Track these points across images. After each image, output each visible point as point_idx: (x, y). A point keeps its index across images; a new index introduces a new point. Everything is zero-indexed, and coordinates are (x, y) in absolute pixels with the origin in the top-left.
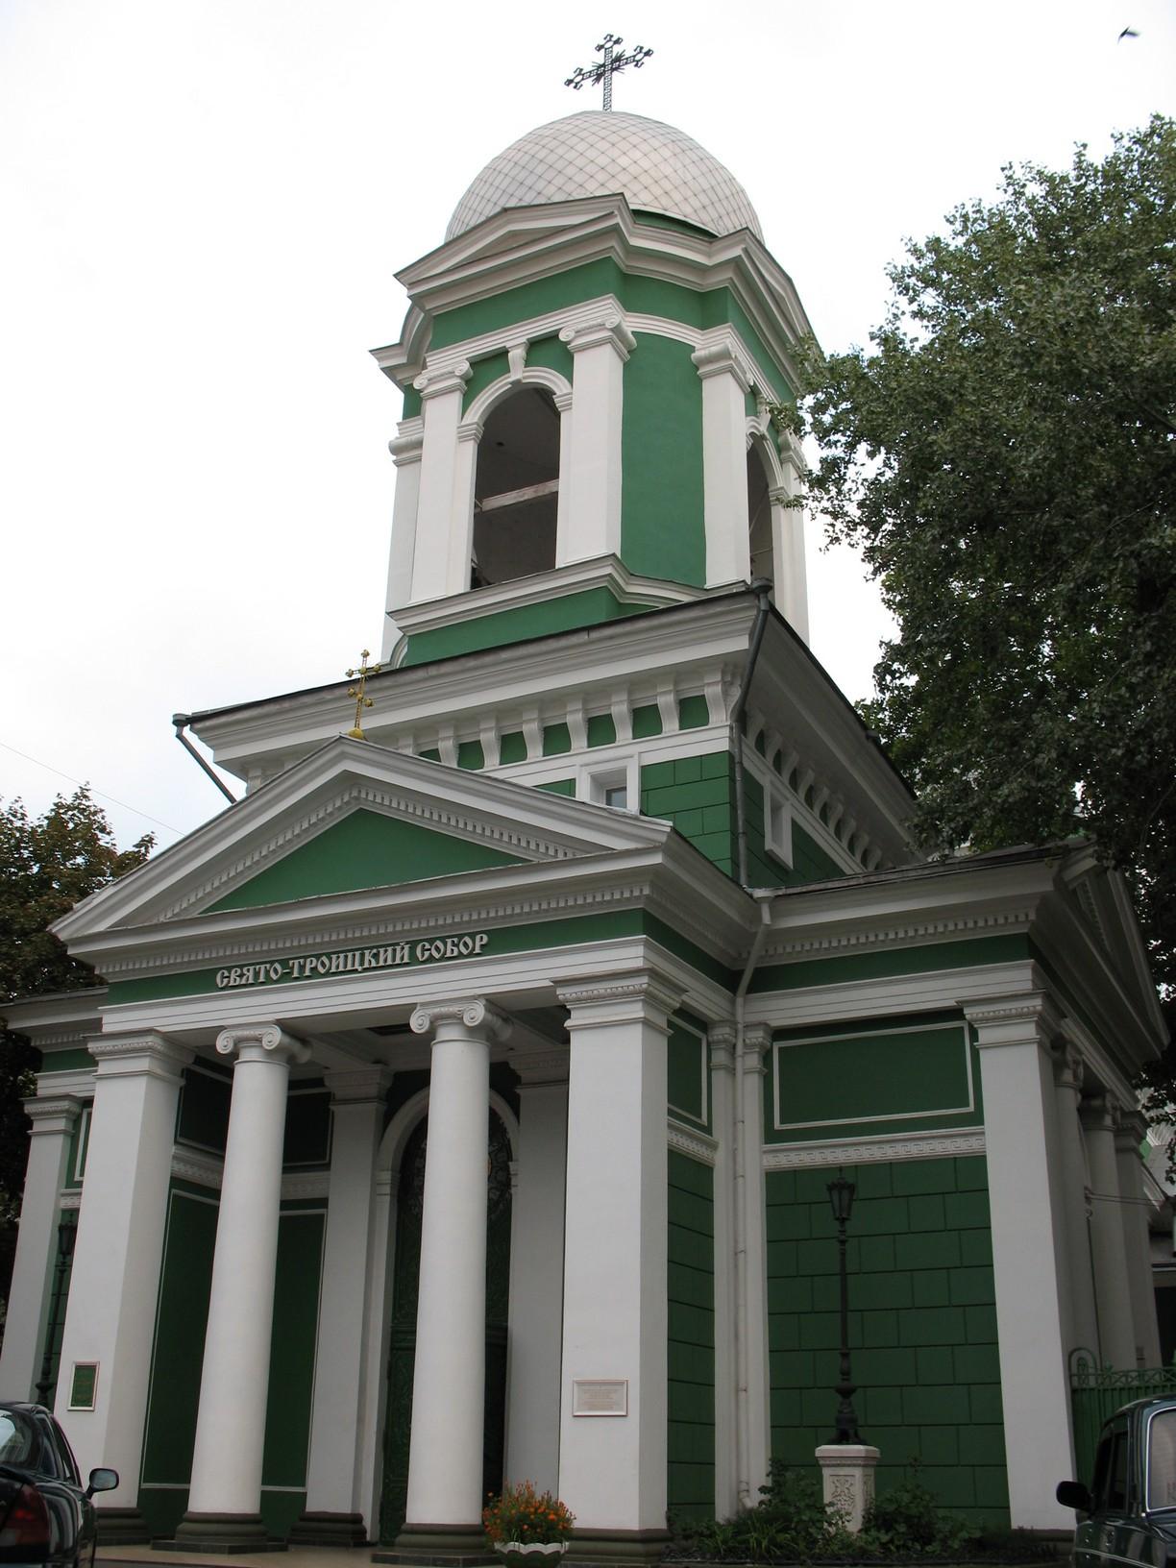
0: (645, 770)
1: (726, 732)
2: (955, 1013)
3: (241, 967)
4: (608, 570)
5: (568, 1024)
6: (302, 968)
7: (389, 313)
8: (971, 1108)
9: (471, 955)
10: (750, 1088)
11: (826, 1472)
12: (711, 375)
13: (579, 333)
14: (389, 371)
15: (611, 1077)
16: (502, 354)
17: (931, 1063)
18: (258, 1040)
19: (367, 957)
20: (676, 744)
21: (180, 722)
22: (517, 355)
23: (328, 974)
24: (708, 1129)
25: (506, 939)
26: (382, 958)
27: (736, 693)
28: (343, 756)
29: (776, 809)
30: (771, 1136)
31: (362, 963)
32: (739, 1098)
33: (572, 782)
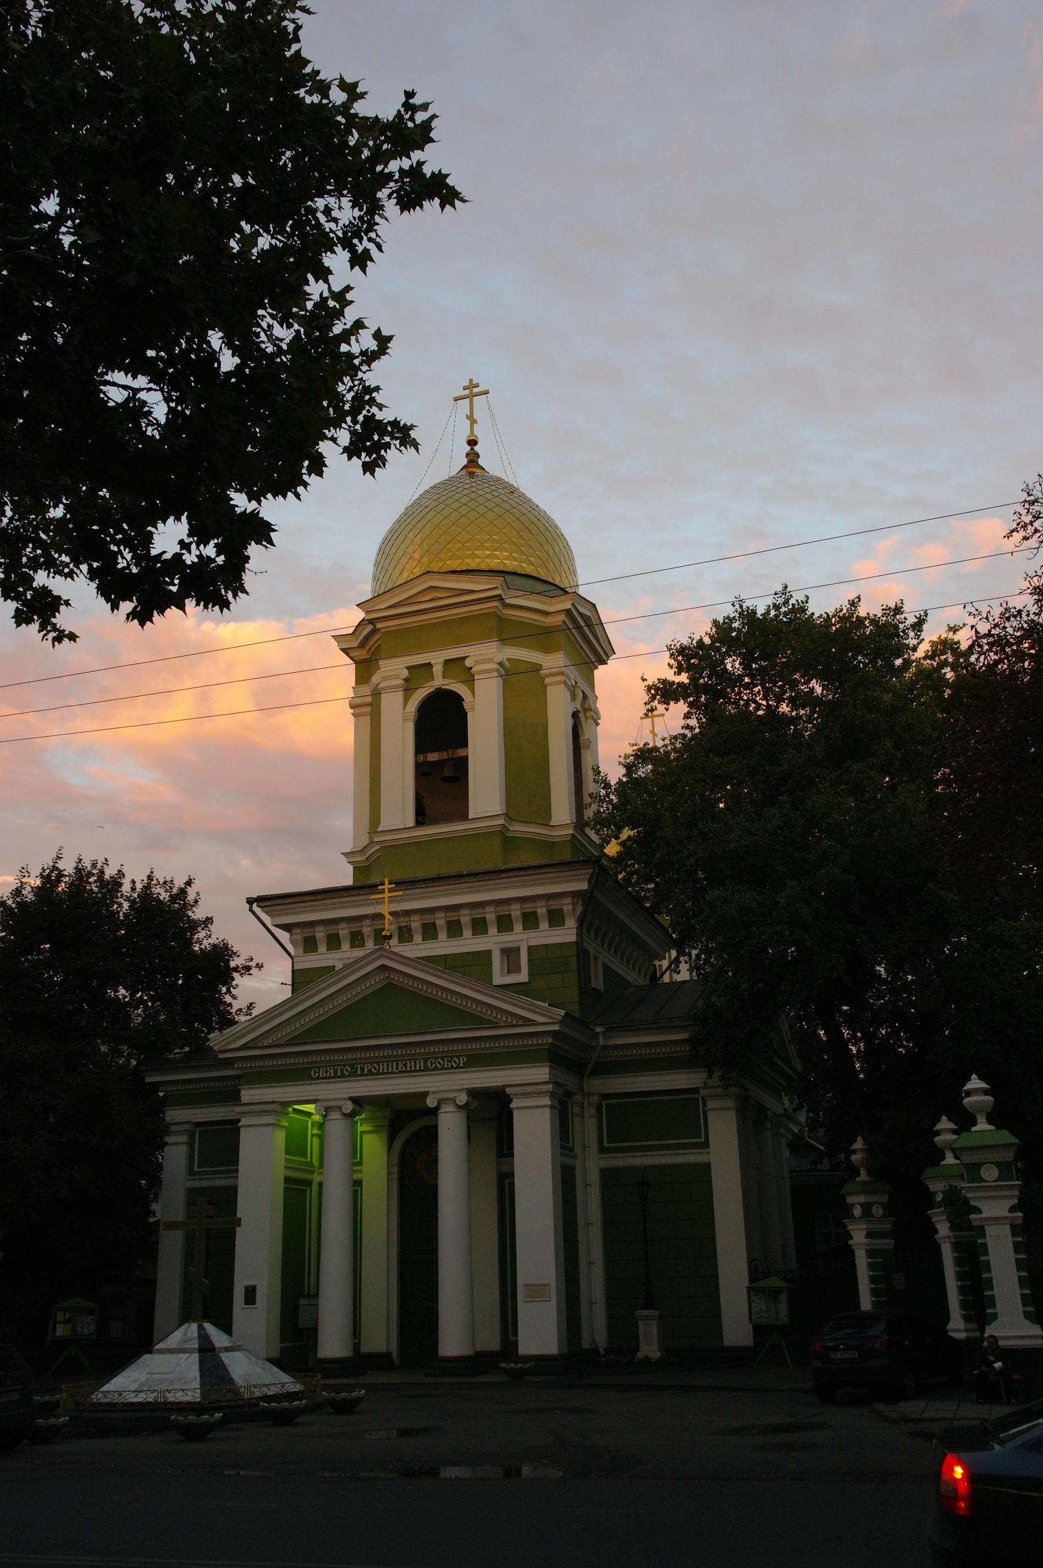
0: (530, 948)
1: (575, 931)
2: (696, 1090)
4: (502, 822)
5: (512, 1105)
6: (362, 1069)
7: (351, 618)
8: (703, 1139)
9: (458, 1067)
10: (592, 1125)
11: (640, 1323)
12: (552, 684)
13: (477, 662)
14: (345, 651)
15: (533, 1129)
16: (429, 666)
17: (682, 1117)
18: (340, 1108)
20: (546, 935)
21: (250, 901)
22: (438, 669)
23: (378, 1073)
24: (572, 1149)
25: (477, 1061)
27: (579, 908)
28: (382, 956)
29: (596, 958)
30: (602, 1150)
31: (397, 1068)
32: (587, 1131)
33: (488, 953)
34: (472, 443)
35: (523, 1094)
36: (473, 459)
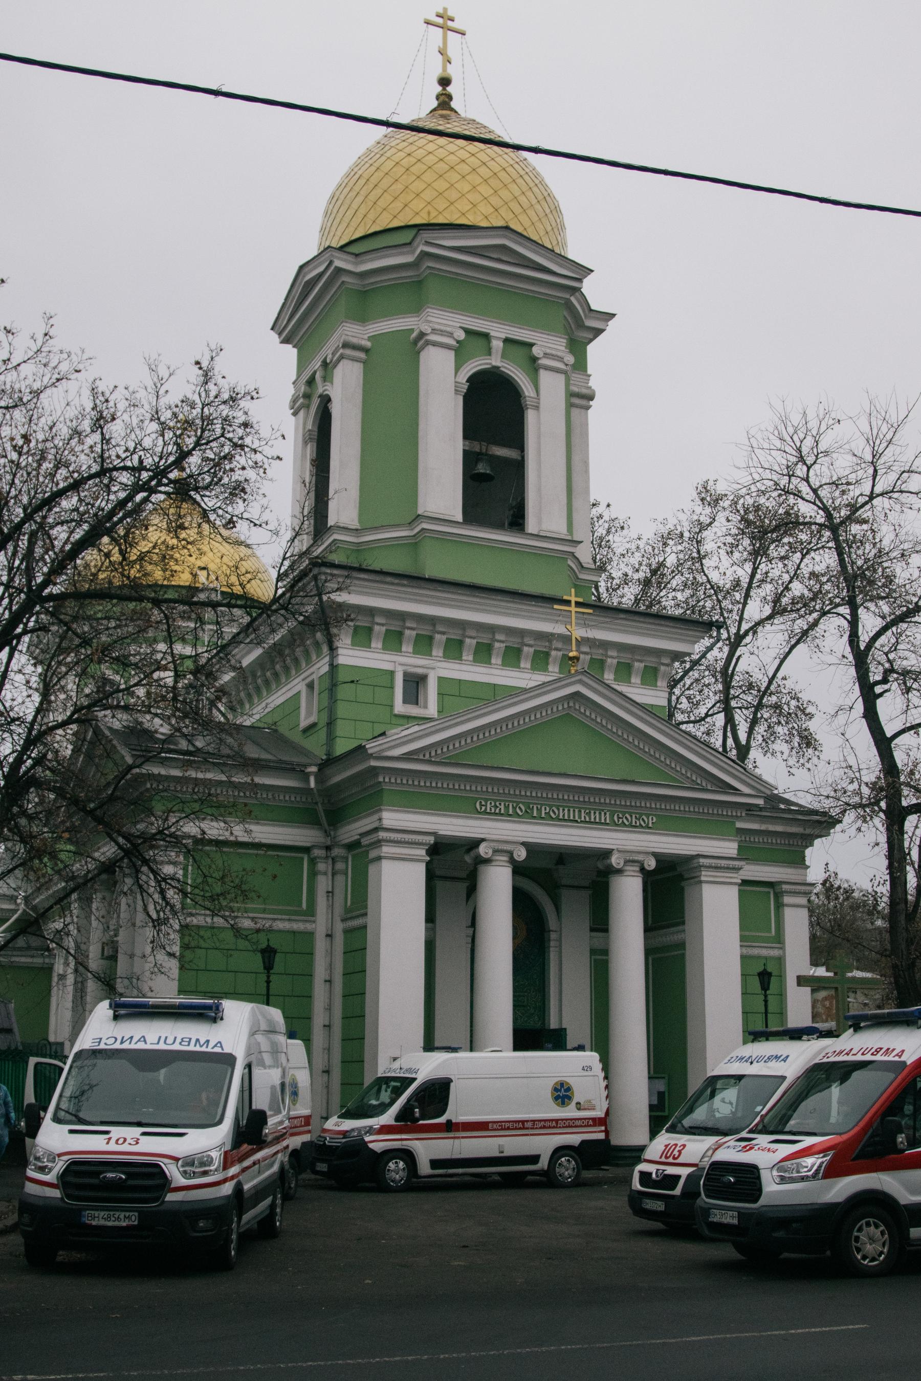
3: (495, 801)
6: (539, 810)
13: (546, 355)
16: (486, 336)
19: (583, 815)
22: (497, 345)
26: (593, 817)
28: (580, 682)
31: (580, 817)
34: (445, 82)
36: (444, 102)
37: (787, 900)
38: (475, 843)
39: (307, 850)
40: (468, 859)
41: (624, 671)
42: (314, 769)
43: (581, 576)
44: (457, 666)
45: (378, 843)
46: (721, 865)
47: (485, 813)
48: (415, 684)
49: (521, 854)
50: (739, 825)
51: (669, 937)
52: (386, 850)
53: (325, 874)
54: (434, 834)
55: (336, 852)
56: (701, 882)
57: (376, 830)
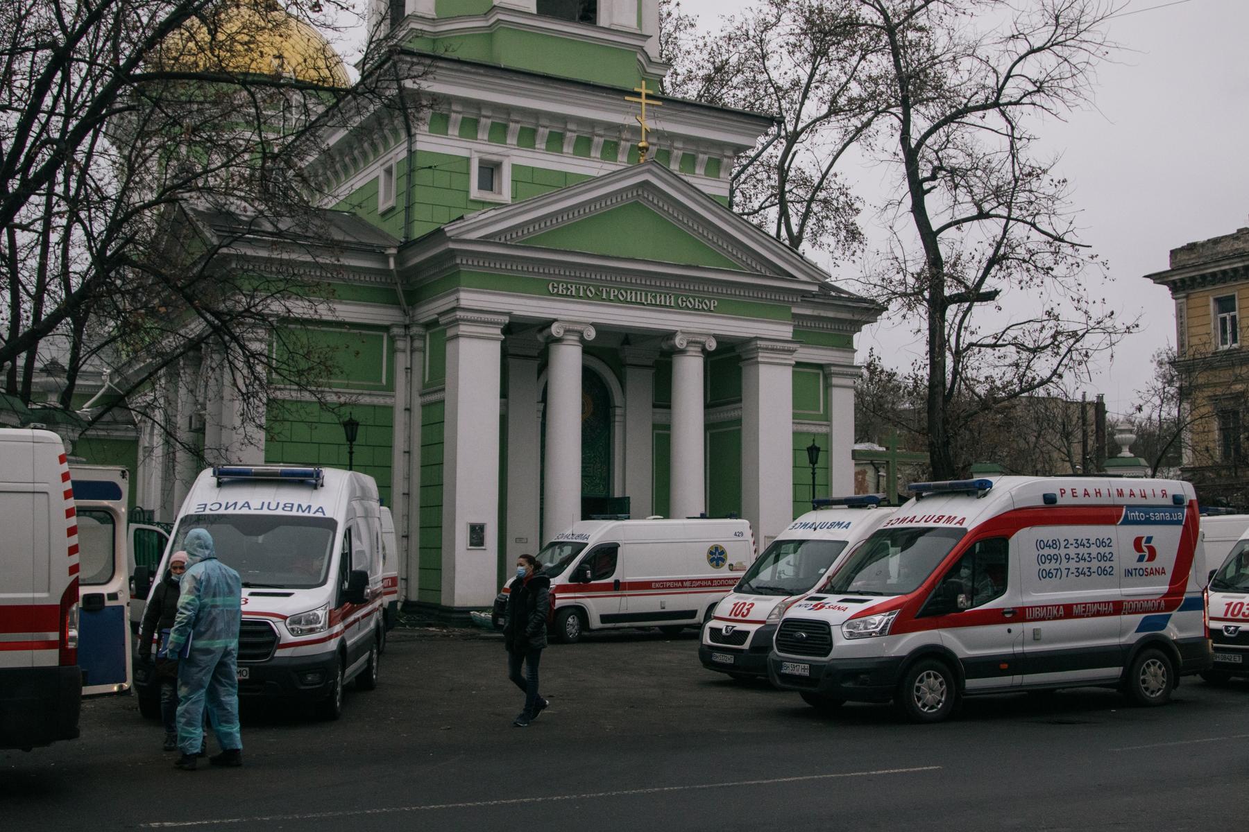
6: (608, 293)
28: (649, 171)
35: (772, 349)
37: (835, 381)
38: (548, 323)
39: (386, 328)
40: (540, 338)
41: (689, 162)
42: (393, 251)
43: (649, 70)
44: (530, 154)
45: (456, 322)
46: (777, 347)
47: (558, 294)
48: (490, 171)
49: (591, 334)
50: (795, 310)
51: (726, 414)
52: (464, 329)
53: (404, 351)
54: (509, 314)
55: (415, 330)
56: (758, 363)
57: (454, 309)
